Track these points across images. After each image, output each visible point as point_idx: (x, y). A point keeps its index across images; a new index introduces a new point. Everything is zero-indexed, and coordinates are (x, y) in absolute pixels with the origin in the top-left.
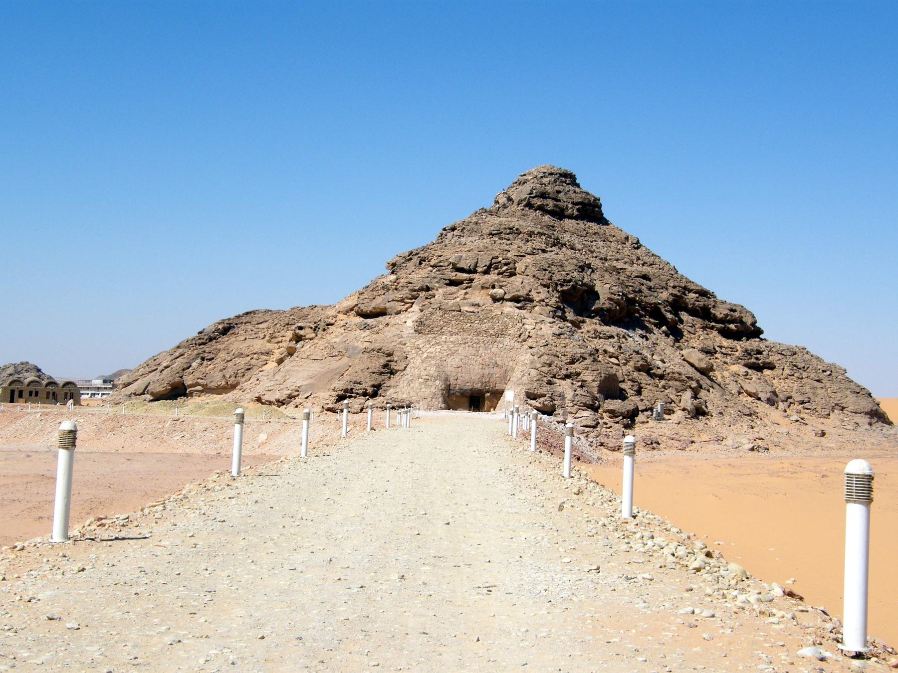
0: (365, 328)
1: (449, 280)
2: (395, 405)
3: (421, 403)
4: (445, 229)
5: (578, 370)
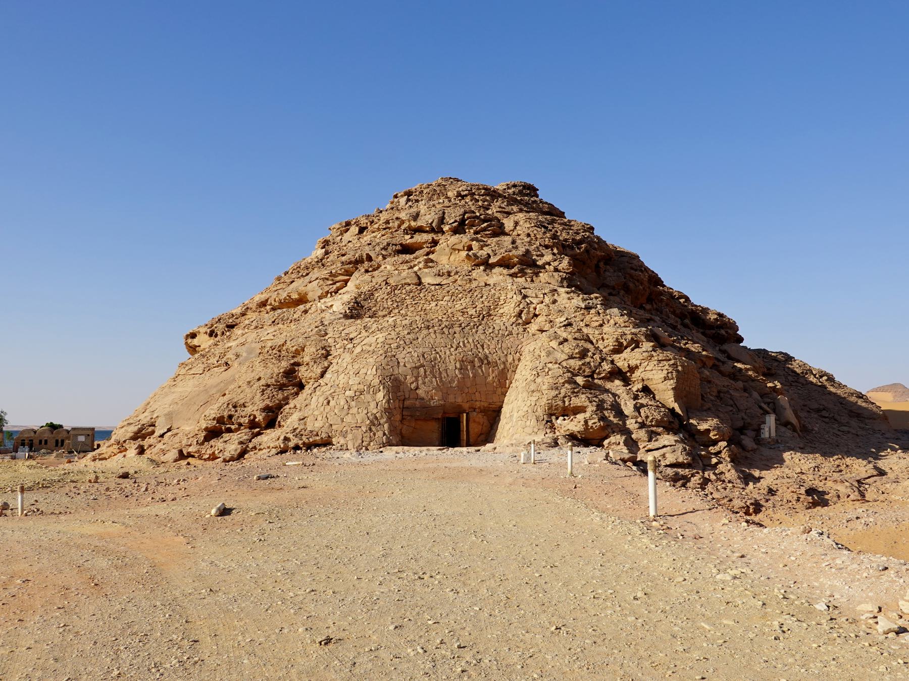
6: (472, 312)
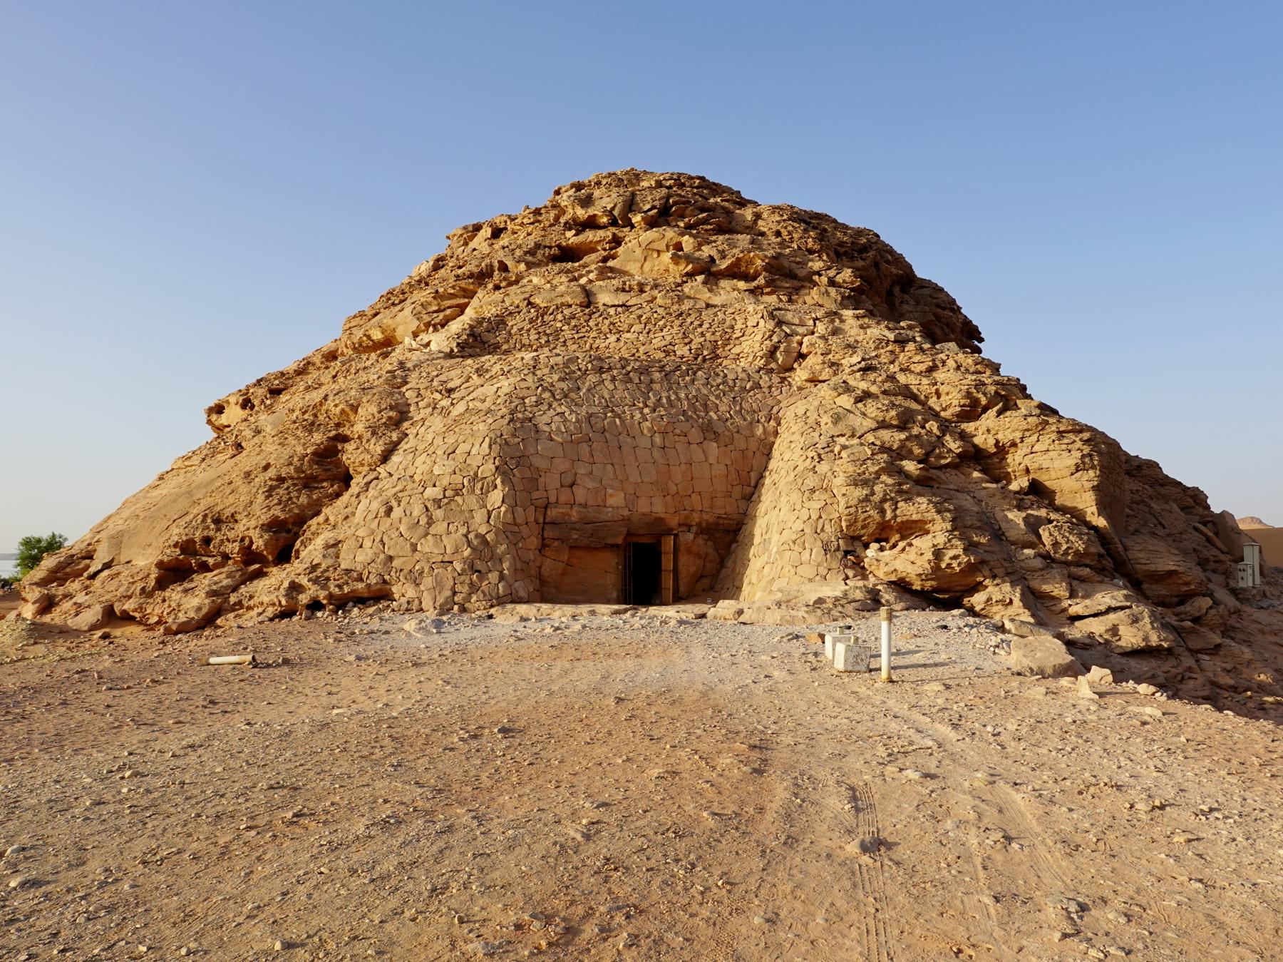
0: (334, 377)
1: (559, 246)
2: (322, 595)
3: (428, 582)
4: (557, 193)
5: (1005, 437)
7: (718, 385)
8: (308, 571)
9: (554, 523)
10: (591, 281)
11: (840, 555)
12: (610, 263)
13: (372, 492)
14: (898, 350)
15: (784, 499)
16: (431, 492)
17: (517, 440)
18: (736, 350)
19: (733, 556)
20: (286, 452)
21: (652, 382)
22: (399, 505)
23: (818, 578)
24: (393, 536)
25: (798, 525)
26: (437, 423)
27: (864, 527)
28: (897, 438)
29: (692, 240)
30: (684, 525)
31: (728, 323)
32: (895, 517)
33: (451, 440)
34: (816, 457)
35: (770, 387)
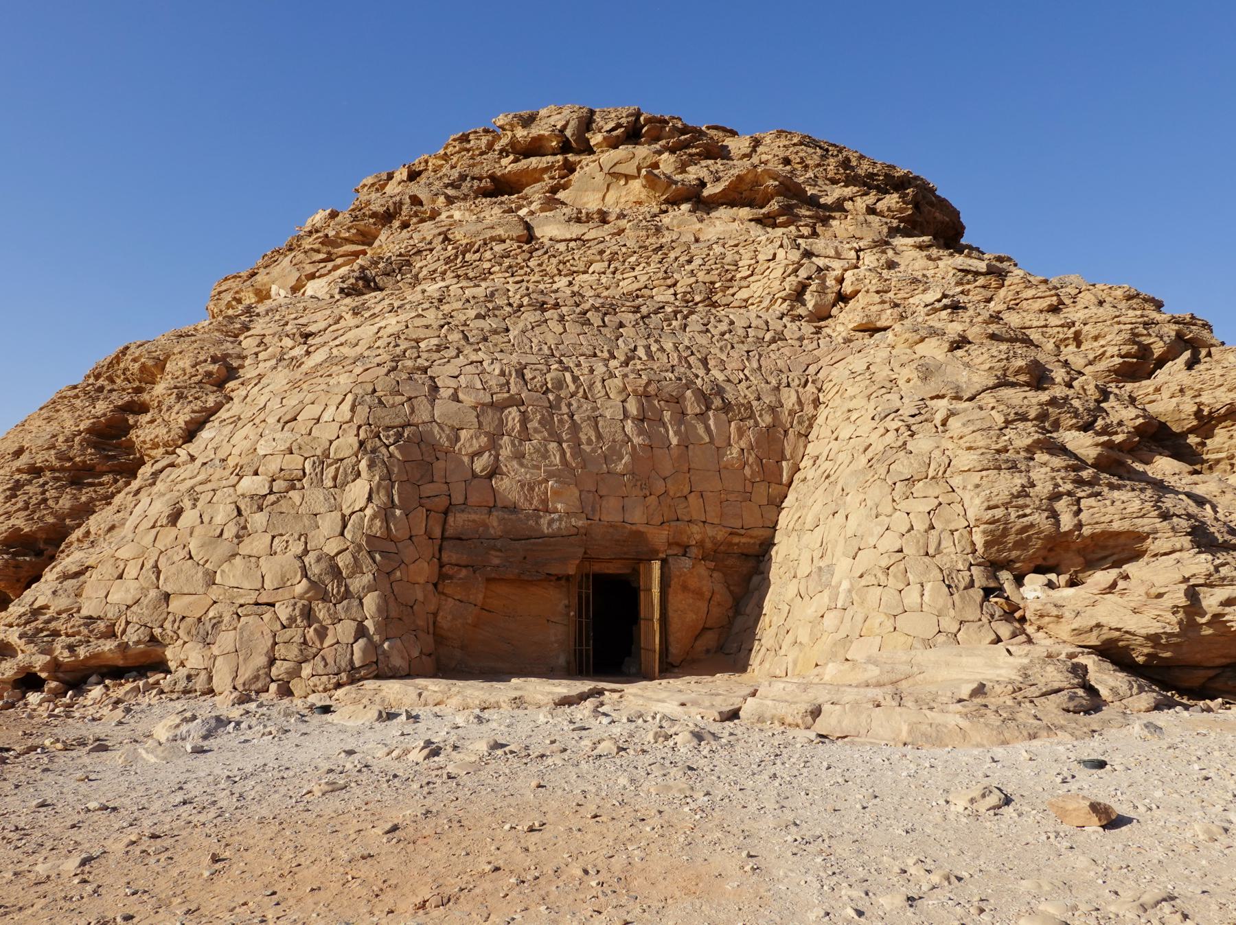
1: (492, 177)
2: (39, 662)
3: (226, 640)
6: (663, 295)
7: (723, 334)
8: (23, 620)
9: (460, 539)
10: (532, 213)
11: (977, 594)
12: (561, 195)
13: (160, 486)
14: (994, 284)
15: (852, 499)
16: (249, 484)
17: (398, 399)
18: (744, 294)
19: (756, 594)
20: (54, 427)
21: (621, 325)
22: (194, 506)
23: (941, 638)
24: (176, 558)
25: (891, 542)
26: (280, 379)
27: (1020, 544)
28: (1034, 401)
29: (672, 158)
30: (678, 544)
31: (728, 259)
32: (1080, 525)
33: (292, 401)
34: (903, 429)
35: (801, 339)
